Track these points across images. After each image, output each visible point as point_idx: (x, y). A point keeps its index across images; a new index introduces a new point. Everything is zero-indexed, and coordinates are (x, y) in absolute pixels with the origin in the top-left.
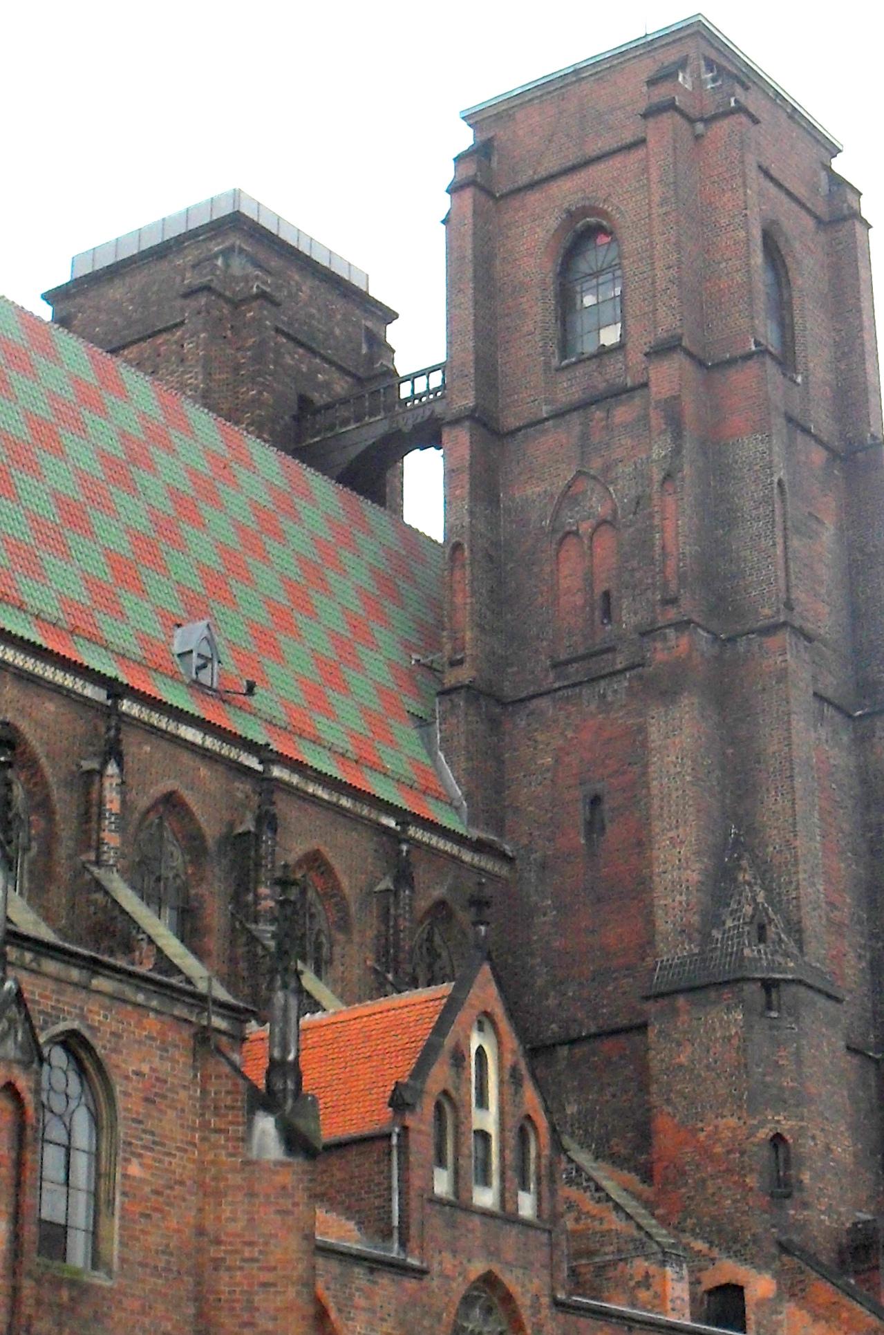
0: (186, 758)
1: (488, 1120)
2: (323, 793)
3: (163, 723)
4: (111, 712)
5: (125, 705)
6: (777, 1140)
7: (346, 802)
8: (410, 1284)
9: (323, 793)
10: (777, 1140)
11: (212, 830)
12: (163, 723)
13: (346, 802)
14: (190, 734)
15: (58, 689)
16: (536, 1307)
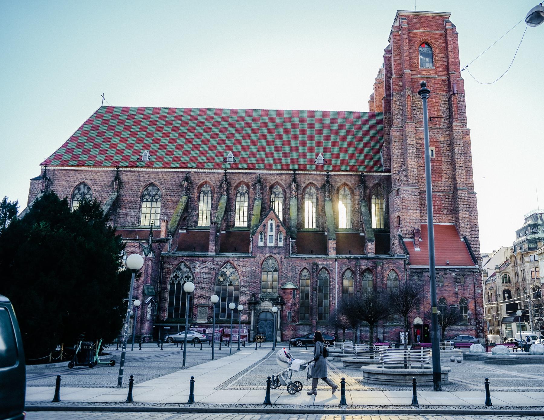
0: (314, 176)
1: (273, 233)
2: (346, 173)
3: (310, 173)
4: (295, 174)
5: (297, 172)
6: (398, 216)
7: (351, 173)
8: (252, 259)
9: (346, 173)
10: (398, 216)
11: (319, 186)
12: (308, 172)
13: (351, 173)
14: (313, 172)
15: (286, 174)
16: (281, 259)
